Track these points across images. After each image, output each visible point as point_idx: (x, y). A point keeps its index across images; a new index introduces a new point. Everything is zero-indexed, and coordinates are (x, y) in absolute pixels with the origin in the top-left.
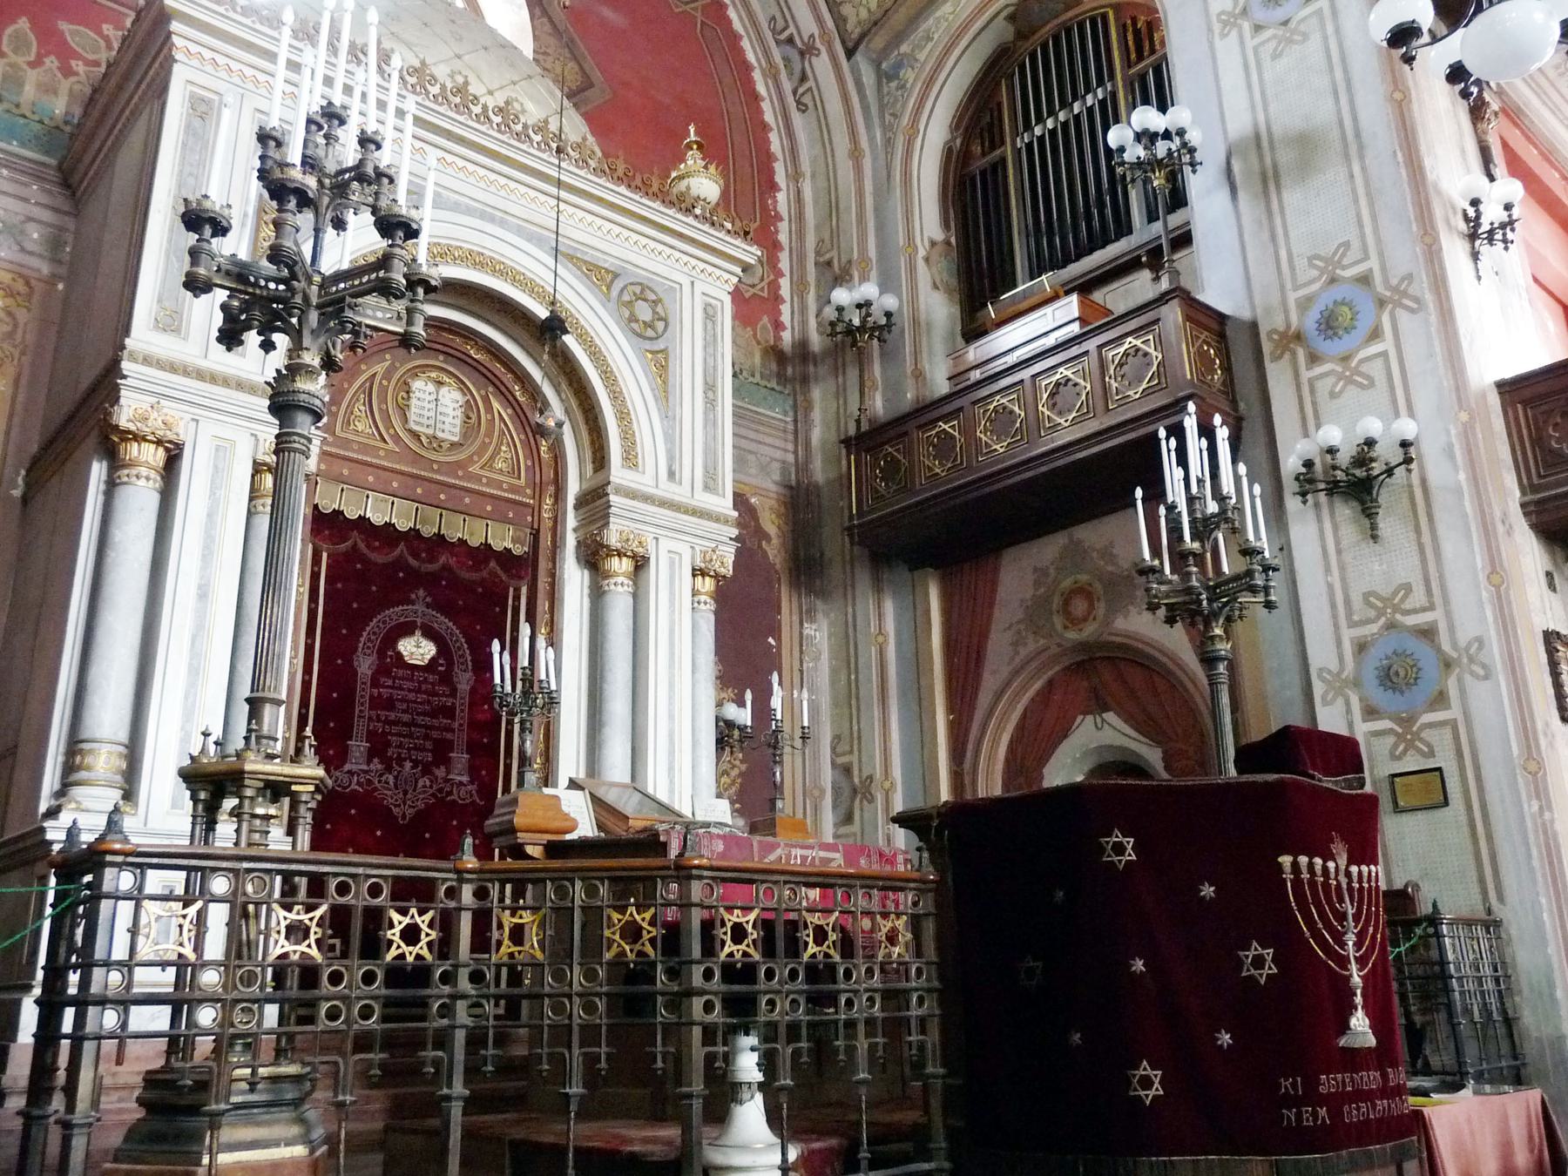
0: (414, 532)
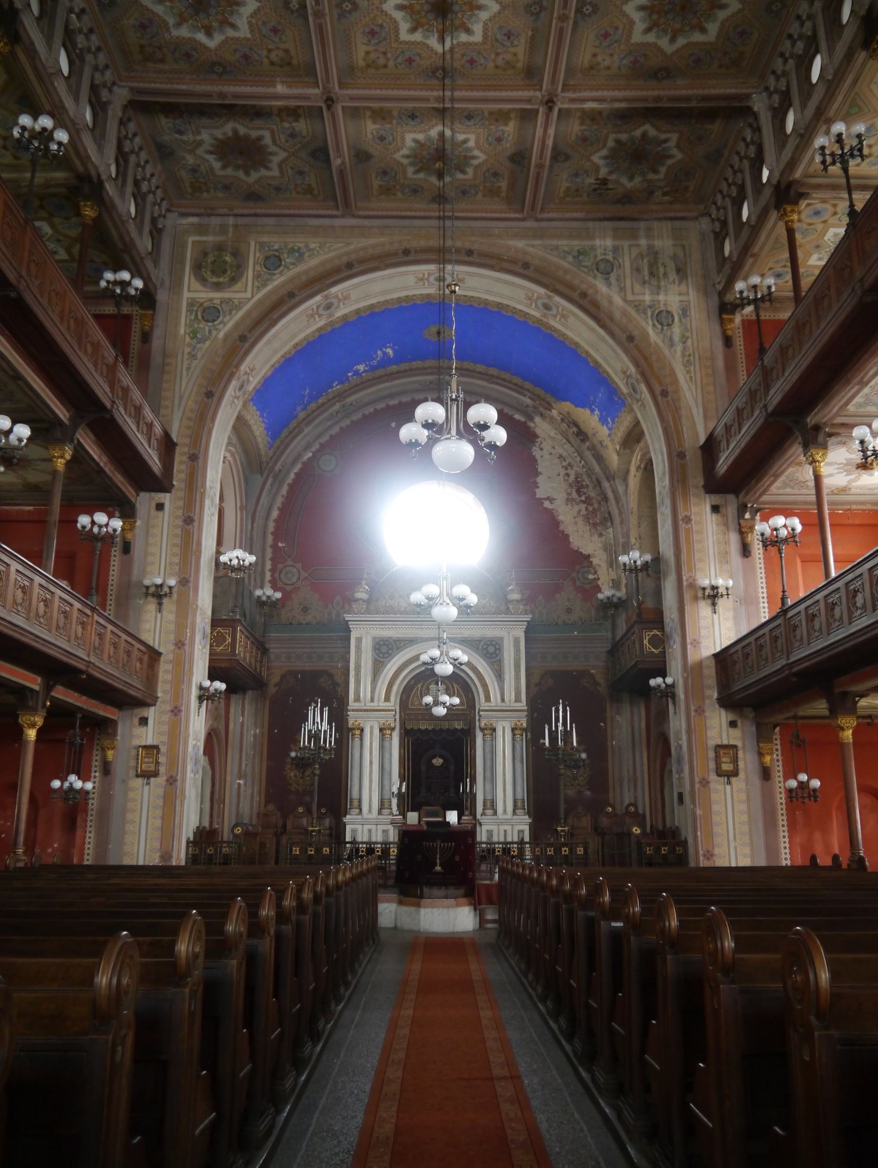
0: (433, 730)
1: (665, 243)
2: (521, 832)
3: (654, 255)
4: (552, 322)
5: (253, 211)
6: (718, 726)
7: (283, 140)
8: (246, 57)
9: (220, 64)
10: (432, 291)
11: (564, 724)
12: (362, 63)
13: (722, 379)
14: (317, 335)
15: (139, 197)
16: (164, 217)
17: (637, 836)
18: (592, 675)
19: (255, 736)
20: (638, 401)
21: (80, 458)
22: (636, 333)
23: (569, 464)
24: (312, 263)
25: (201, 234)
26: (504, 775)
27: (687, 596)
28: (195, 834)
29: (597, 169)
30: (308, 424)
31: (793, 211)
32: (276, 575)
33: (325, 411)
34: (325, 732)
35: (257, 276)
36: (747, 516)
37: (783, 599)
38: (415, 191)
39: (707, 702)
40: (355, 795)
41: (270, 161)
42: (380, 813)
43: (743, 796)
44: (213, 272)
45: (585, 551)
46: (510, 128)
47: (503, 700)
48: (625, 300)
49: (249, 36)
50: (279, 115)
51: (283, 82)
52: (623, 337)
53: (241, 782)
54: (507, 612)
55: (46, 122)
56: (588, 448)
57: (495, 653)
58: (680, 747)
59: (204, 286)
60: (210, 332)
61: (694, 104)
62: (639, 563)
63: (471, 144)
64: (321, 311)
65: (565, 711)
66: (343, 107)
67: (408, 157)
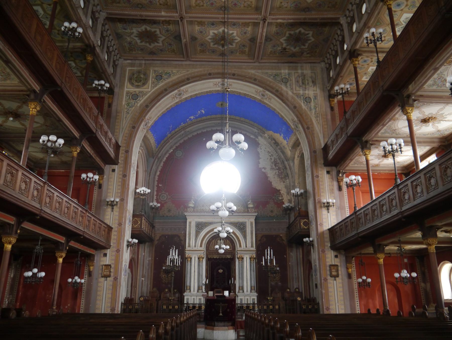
1: (308, 72)
2: (253, 299)
3: (304, 76)
4: (265, 101)
5: (152, 58)
6: (330, 257)
7: (164, 32)
9: (141, 4)
10: (219, 89)
11: (270, 256)
12: (194, 5)
13: (330, 123)
14: (175, 105)
15: (109, 53)
16: (118, 60)
17: (299, 301)
18: (281, 237)
19: (149, 260)
20: (298, 131)
21: (83, 151)
22: (297, 105)
23: (272, 155)
24: (174, 78)
25: (132, 67)
26: (247, 276)
27: (318, 206)
28: (124, 300)
29: (282, 44)
30: (172, 139)
31: (356, 60)
32: (158, 197)
33: (178, 134)
34: (177, 259)
35: (153, 83)
36: (340, 175)
37: (355, 208)
38: (213, 52)
39: (326, 248)
40: (188, 284)
41: (159, 40)
42: (198, 292)
43: (341, 285)
44: (136, 81)
45: (278, 188)
46: (249, 29)
47: (246, 247)
48: (293, 93)
50: (162, 23)
51: (164, 11)
52: (292, 107)
53: (143, 279)
54: (248, 212)
55: (74, 25)
56: (279, 149)
57: (243, 228)
58: (316, 265)
59: (133, 86)
60: (134, 104)
61: (318, 21)
62: (299, 193)
63: (235, 34)
64: (177, 96)
65: (270, 251)
66: (187, 21)
67: (211, 39)
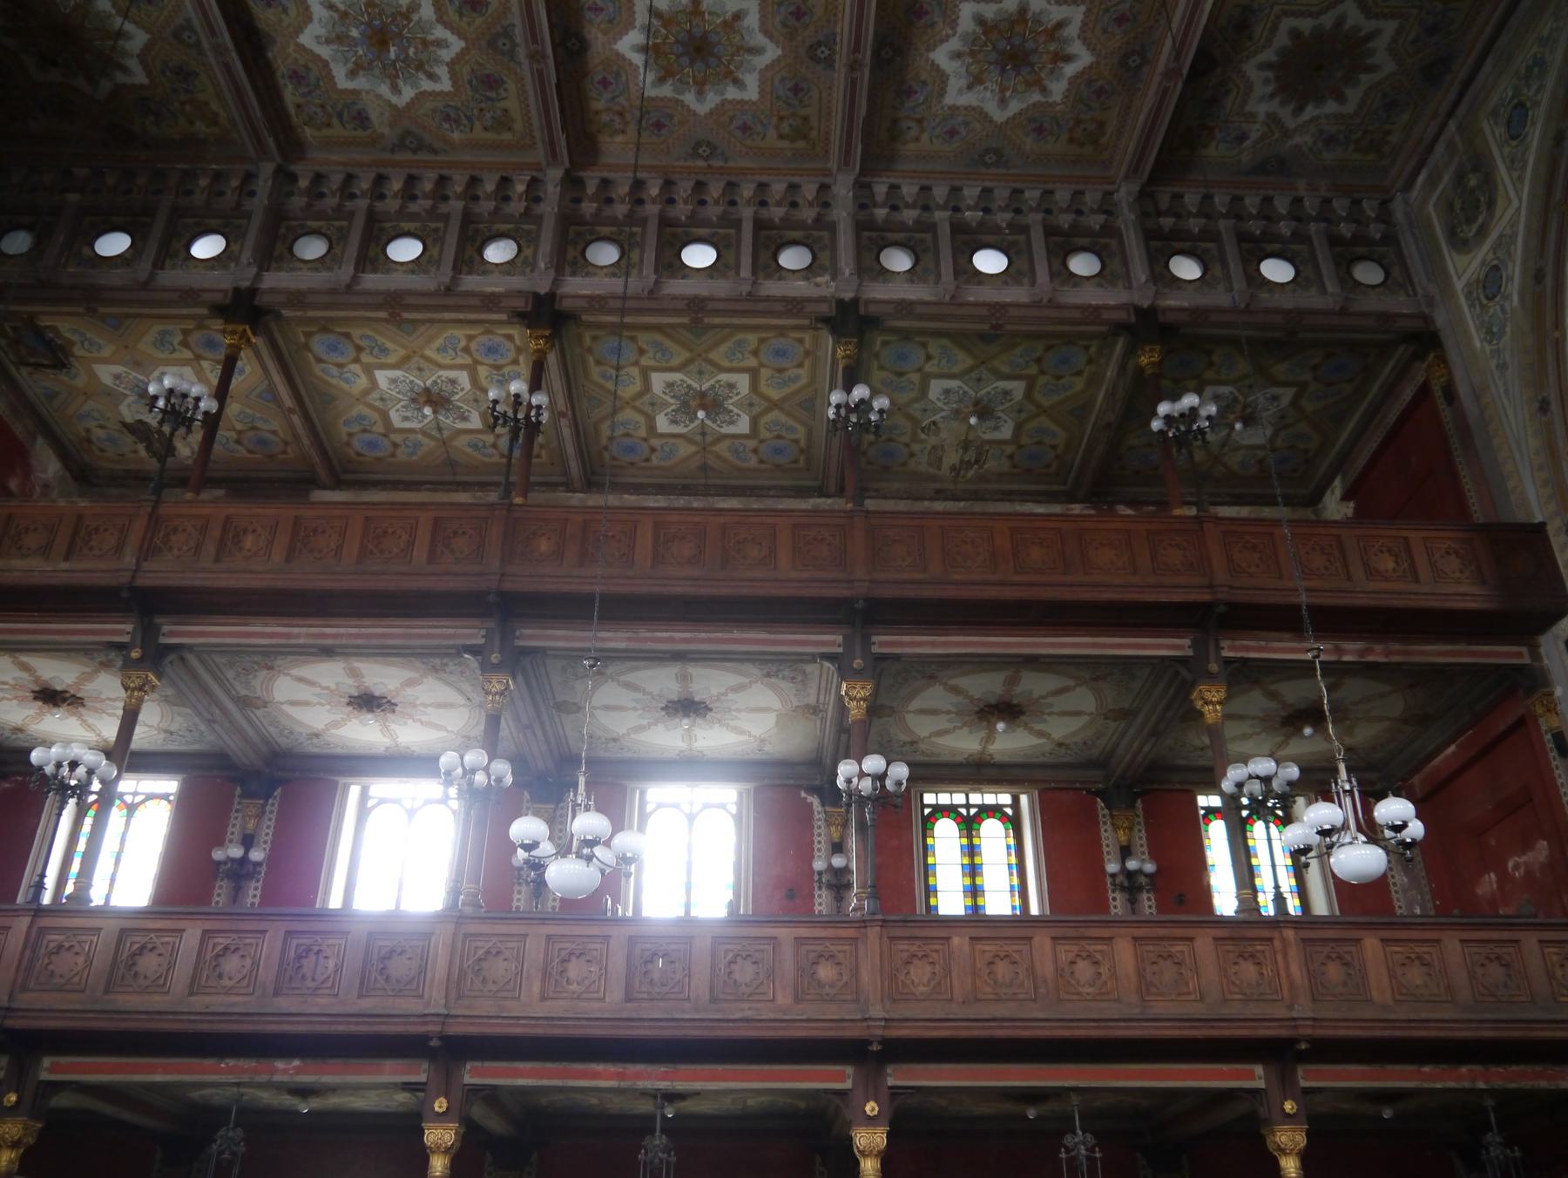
8: (1121, 20)
49: (1083, 8)
